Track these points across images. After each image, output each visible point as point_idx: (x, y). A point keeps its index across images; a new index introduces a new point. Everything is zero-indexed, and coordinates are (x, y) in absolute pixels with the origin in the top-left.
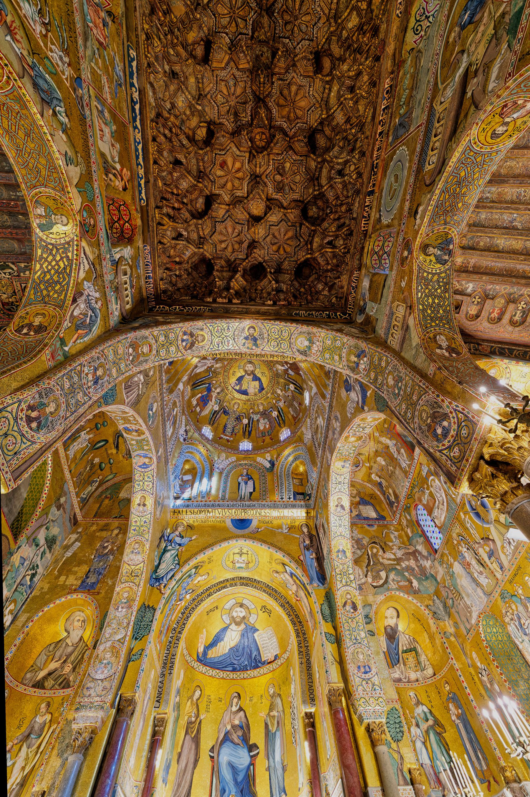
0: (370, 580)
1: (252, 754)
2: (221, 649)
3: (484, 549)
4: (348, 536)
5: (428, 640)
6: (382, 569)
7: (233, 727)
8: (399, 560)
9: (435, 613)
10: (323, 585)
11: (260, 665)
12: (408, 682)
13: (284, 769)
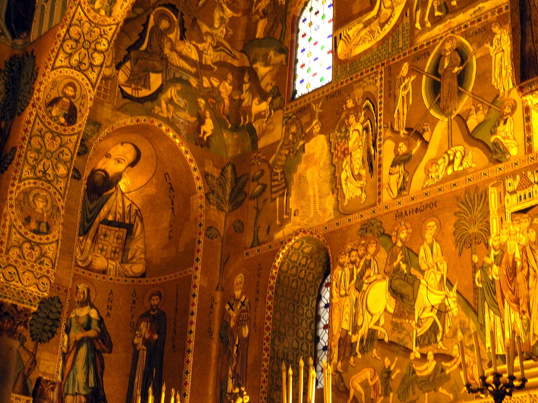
0: (122, 77)
3: (397, 147)
5: (166, 224)
6: (159, 67)
9: (213, 192)
10: (14, 37)
12: (87, 268)
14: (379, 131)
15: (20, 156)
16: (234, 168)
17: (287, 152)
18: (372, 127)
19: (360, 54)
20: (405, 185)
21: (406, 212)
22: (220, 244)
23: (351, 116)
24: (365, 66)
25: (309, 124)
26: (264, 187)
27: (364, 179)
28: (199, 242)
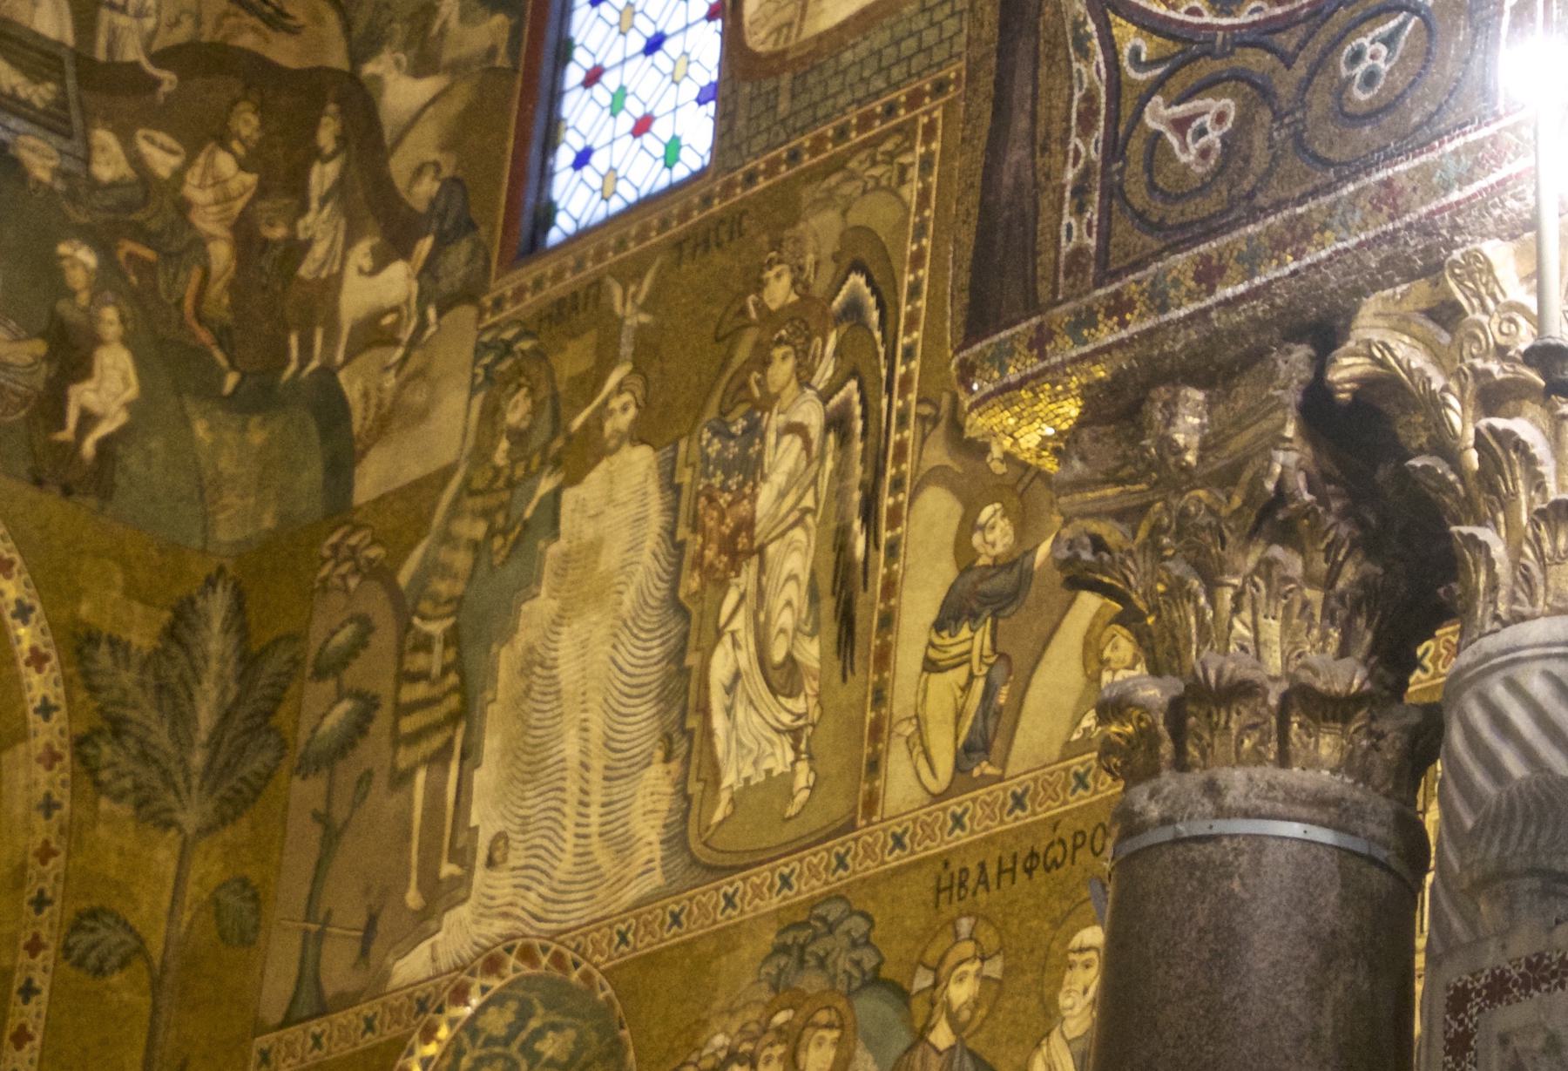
3: (969, 524)
9: (118, 728)
14: (895, 437)
16: (239, 605)
17: (479, 529)
18: (864, 416)
19: (842, 27)
20: (991, 723)
21: (982, 866)
22: (144, 1003)
23: (778, 353)
24: (860, 94)
25: (590, 383)
26: (368, 706)
27: (811, 686)
28: (28, 991)
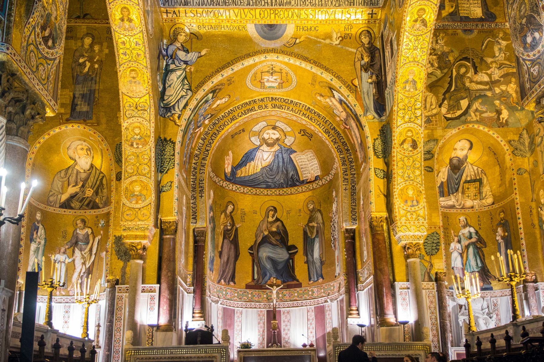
0: (444, 110)
1: (290, 252)
2: (251, 168)
4: (424, 63)
7: (271, 233)
8: (493, 83)
10: (380, 116)
11: (297, 183)
13: (322, 263)
15: (394, 174)
